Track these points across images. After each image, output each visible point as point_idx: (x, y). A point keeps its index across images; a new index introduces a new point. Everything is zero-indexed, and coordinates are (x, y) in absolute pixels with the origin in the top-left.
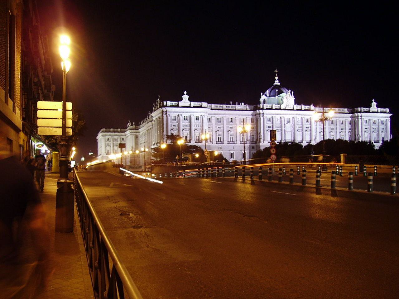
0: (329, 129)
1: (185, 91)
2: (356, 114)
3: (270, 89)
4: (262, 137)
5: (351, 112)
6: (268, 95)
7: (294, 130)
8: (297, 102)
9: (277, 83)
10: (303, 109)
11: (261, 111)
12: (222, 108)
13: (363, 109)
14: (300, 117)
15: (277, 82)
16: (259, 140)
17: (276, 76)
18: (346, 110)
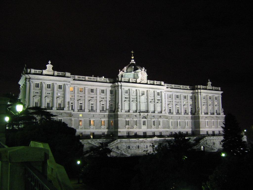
0: (175, 102)
1: (50, 61)
2: (196, 90)
3: (127, 66)
4: (120, 107)
5: (192, 89)
6: (125, 71)
7: (147, 102)
8: (149, 78)
9: (133, 61)
10: (155, 83)
11: (119, 83)
12: (84, 79)
13: (202, 87)
14: (152, 91)
15: (133, 61)
16: (117, 109)
17: (132, 56)
18: (188, 87)
